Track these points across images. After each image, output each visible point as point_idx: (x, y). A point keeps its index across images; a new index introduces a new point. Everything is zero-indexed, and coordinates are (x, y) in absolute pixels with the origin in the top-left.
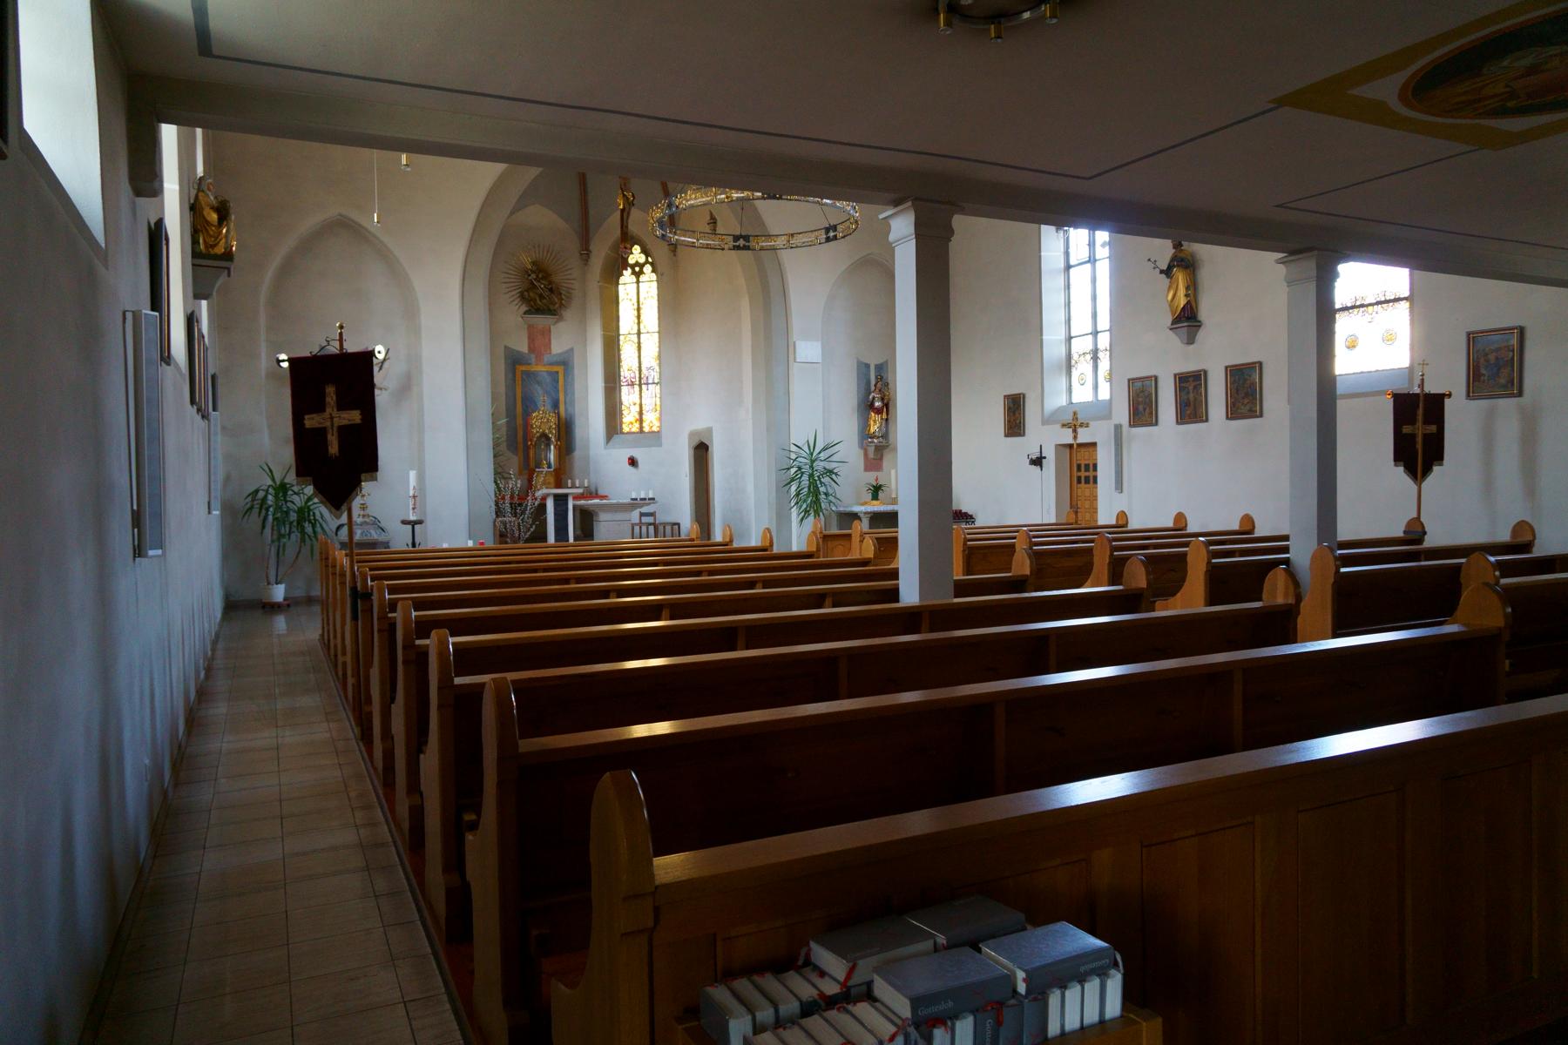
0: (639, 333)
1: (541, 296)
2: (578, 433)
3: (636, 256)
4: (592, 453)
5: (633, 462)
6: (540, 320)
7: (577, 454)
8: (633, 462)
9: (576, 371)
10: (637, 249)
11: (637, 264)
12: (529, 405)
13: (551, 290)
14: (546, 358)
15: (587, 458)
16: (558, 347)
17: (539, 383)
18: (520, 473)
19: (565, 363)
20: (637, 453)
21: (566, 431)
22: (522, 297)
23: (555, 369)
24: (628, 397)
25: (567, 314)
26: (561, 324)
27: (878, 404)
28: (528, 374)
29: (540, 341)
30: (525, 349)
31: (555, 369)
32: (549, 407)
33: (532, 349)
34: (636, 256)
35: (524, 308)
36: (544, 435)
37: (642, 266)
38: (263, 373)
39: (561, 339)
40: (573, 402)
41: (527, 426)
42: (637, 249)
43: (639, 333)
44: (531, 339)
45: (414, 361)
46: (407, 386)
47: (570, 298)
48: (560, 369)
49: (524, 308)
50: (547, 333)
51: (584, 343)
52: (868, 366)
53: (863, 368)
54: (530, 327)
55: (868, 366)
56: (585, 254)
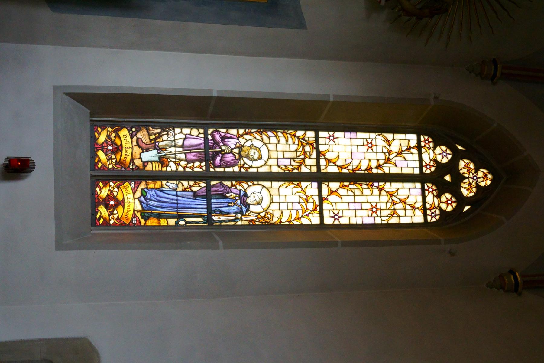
0: (320, 177)
3: (475, 178)
4: (45, 51)
5: (18, 168)
8: (18, 168)
9: (251, 31)
10: (485, 178)
11: (459, 178)
15: (31, 37)
20: (40, 183)
24: (182, 140)
34: (475, 178)
37: (454, 188)
42: (485, 178)
43: (320, 177)
56: (491, 71)
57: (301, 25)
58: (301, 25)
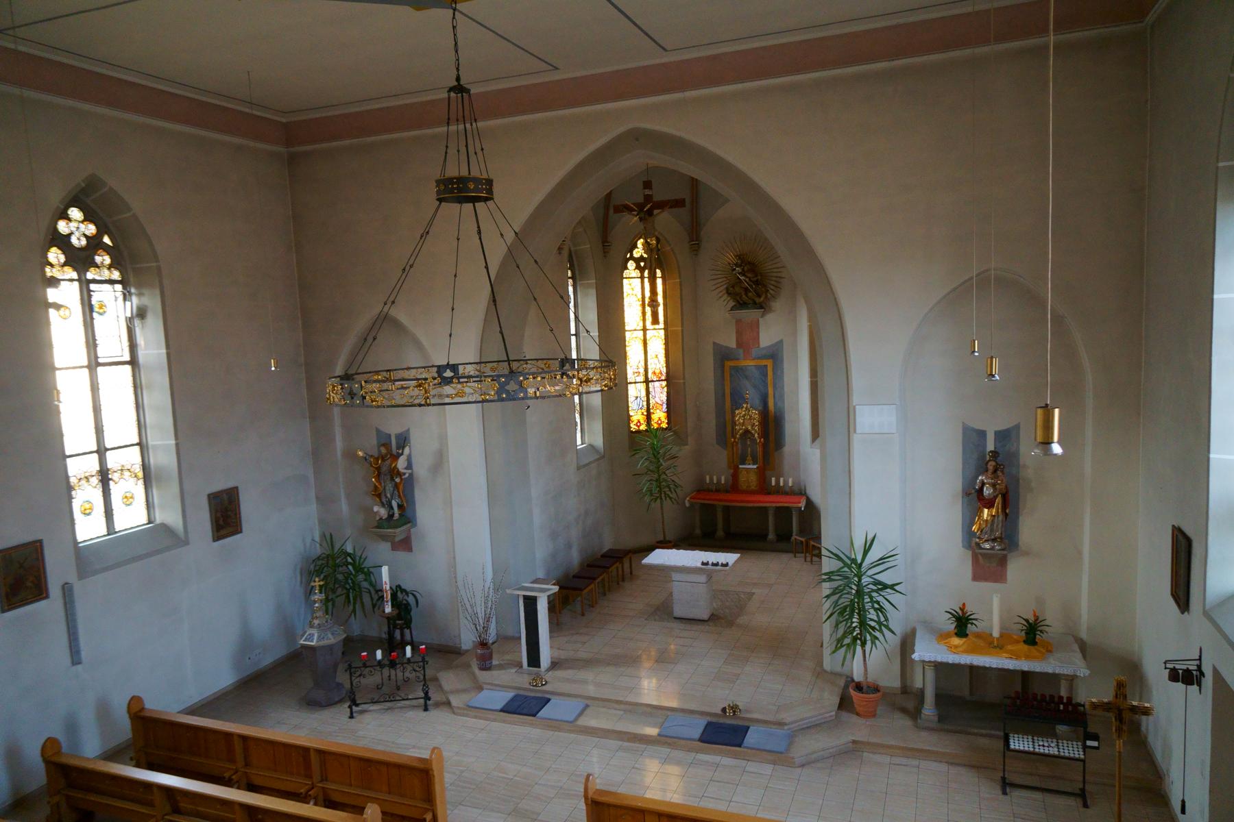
1: (746, 290)
2: (788, 428)
6: (749, 314)
7: (787, 449)
9: (786, 365)
12: (737, 400)
13: (757, 283)
14: (754, 352)
16: (766, 339)
17: (747, 377)
18: (729, 467)
19: (775, 354)
21: (772, 426)
22: (729, 294)
23: (764, 362)
25: (777, 305)
26: (770, 317)
27: (987, 491)
28: (738, 370)
29: (747, 337)
30: (733, 345)
31: (764, 362)
32: (757, 402)
33: (740, 344)
35: (732, 303)
36: (747, 431)
38: (339, 453)
39: (769, 332)
40: (782, 396)
41: (734, 423)
44: (739, 334)
45: (443, 438)
46: (439, 463)
47: (778, 287)
48: (769, 363)
49: (732, 303)
50: (755, 326)
51: (794, 334)
52: (982, 434)
53: (973, 437)
54: (738, 322)
55: (982, 434)
57: (781, 341)
58: (781, 341)
